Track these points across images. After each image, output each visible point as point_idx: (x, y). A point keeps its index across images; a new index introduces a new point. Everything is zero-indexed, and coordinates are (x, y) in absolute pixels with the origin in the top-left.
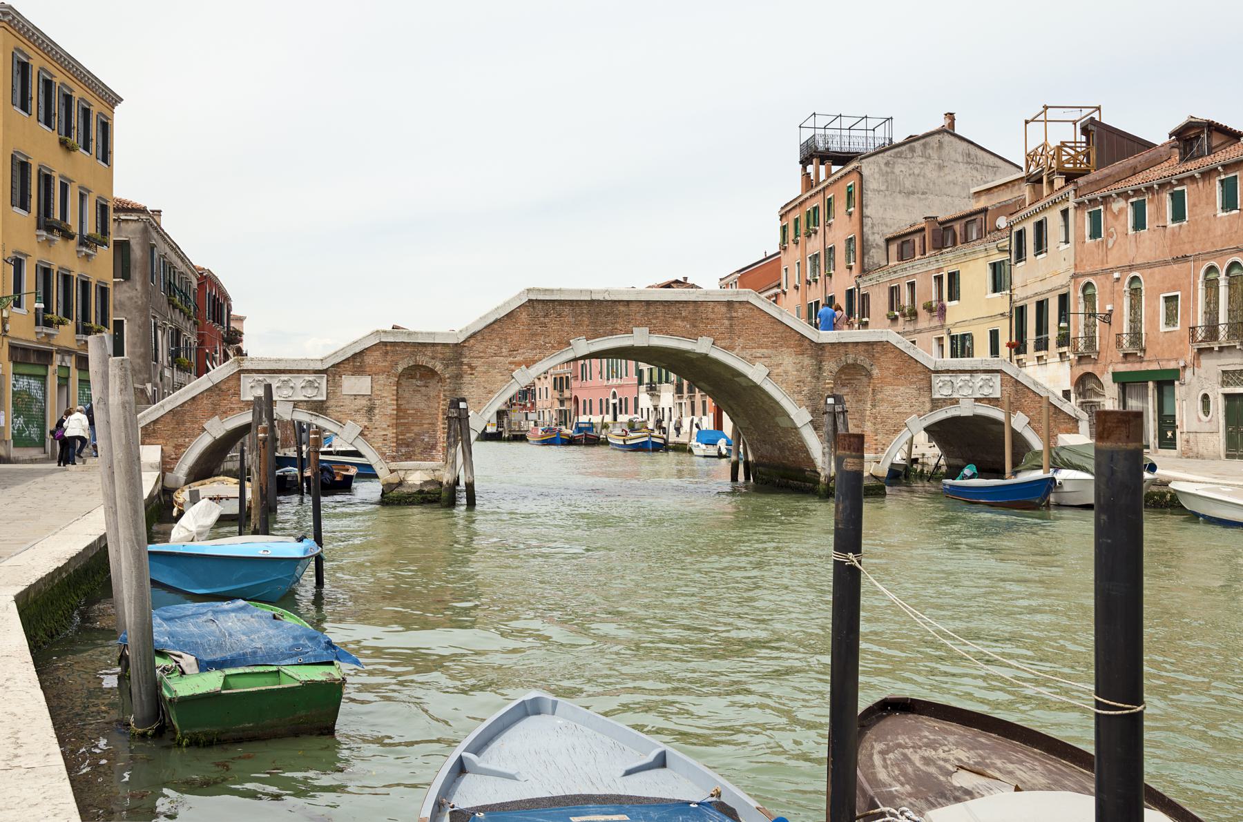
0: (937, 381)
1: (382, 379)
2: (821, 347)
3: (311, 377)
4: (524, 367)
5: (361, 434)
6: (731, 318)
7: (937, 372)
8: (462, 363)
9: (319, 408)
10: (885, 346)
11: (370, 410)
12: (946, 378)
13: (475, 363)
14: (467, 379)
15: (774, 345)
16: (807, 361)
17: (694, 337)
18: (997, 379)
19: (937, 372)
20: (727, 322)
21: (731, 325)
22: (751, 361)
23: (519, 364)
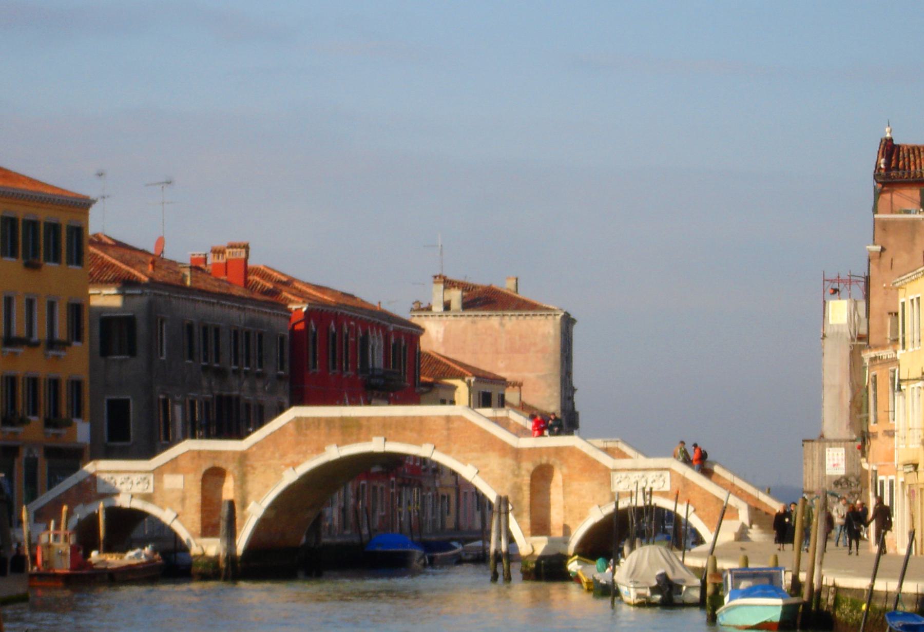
0: (616, 477)
1: (191, 477)
2: (517, 454)
3: (143, 476)
4: (291, 468)
5: (177, 516)
6: (449, 429)
7: (615, 470)
8: (247, 466)
9: (148, 498)
10: (572, 450)
11: (183, 500)
12: (624, 474)
13: (257, 464)
14: (250, 477)
15: (483, 450)
16: (509, 461)
17: (418, 443)
18: (667, 475)
19: (615, 470)
20: (445, 433)
21: (449, 435)
22: (465, 462)
23: (287, 466)
